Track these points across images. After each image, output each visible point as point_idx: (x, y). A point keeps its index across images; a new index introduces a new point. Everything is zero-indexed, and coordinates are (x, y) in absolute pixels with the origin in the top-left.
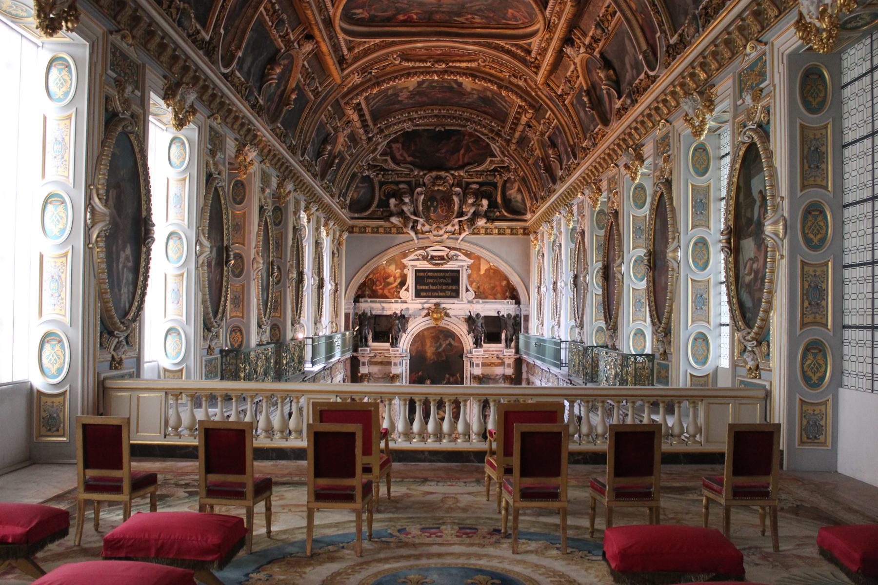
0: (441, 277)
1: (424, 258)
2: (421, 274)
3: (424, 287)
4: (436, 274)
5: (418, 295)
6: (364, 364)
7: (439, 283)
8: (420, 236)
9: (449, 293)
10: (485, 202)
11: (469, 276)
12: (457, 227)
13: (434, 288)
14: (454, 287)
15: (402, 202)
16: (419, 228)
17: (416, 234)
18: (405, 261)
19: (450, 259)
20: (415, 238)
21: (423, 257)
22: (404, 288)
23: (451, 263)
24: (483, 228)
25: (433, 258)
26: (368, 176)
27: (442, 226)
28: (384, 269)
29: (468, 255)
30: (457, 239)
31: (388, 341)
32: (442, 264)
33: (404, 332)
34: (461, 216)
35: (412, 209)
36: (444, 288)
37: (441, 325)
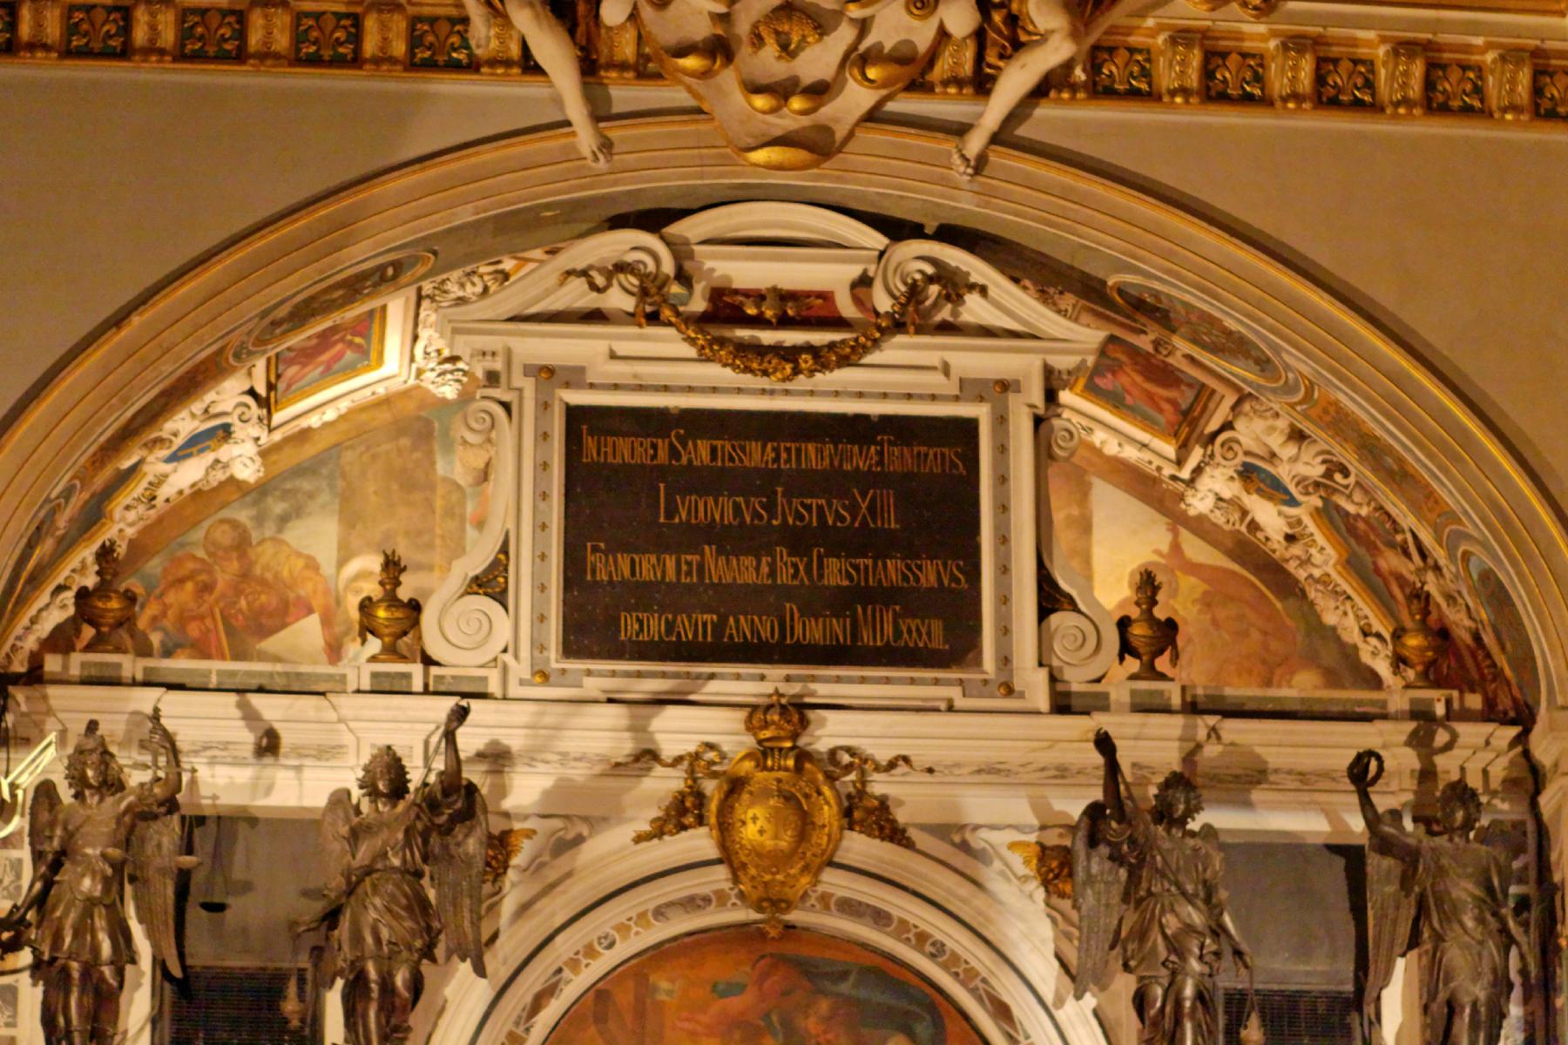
0: (805, 483)
2: (625, 451)
3: (648, 566)
4: (757, 455)
8: (625, 94)
9: (884, 628)
13: (746, 571)
14: (929, 574)
17: (590, 67)
20: (575, 109)
23: (898, 349)
24: (1182, 37)
28: (242, 544)
30: (960, 130)
32: (822, 358)
36: (835, 573)
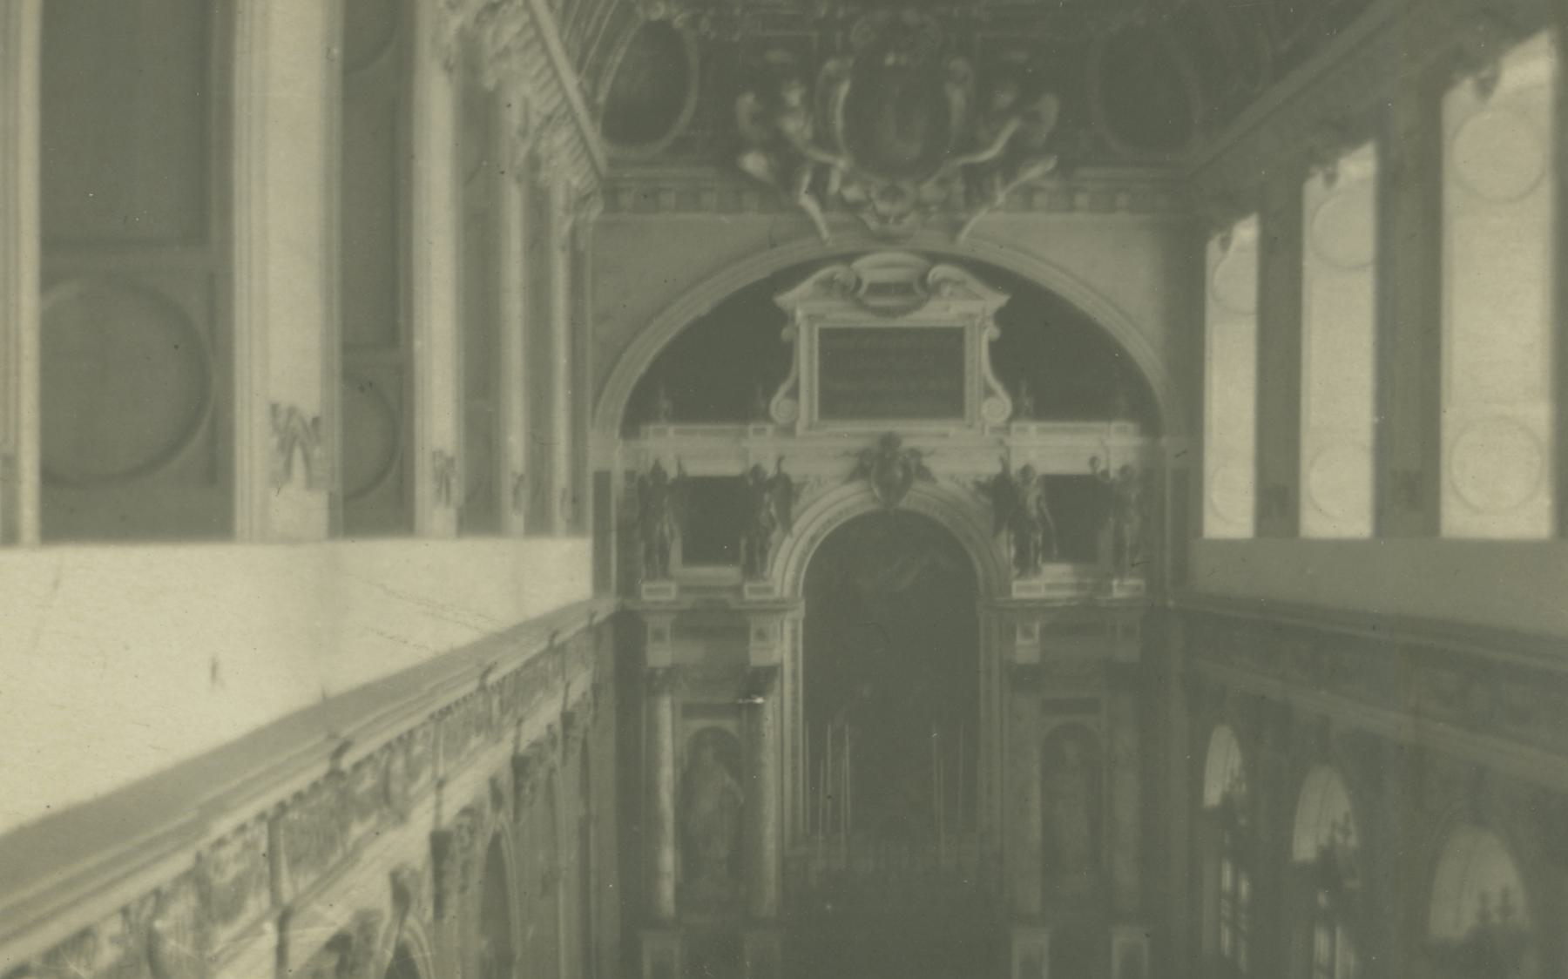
1: (850, 291)
5: (833, 405)
6: (659, 636)
7: (893, 371)
10: (1049, 106)
11: (994, 346)
12: (959, 187)
15: (773, 106)
16: (834, 185)
18: (785, 299)
19: (933, 290)
21: (844, 287)
22: (783, 389)
25: (878, 289)
26: (665, 24)
27: (906, 185)
29: (991, 275)
30: (957, 227)
31: (732, 559)
32: (906, 311)
33: (788, 526)
34: (973, 145)
35: (808, 133)
37: (903, 504)
